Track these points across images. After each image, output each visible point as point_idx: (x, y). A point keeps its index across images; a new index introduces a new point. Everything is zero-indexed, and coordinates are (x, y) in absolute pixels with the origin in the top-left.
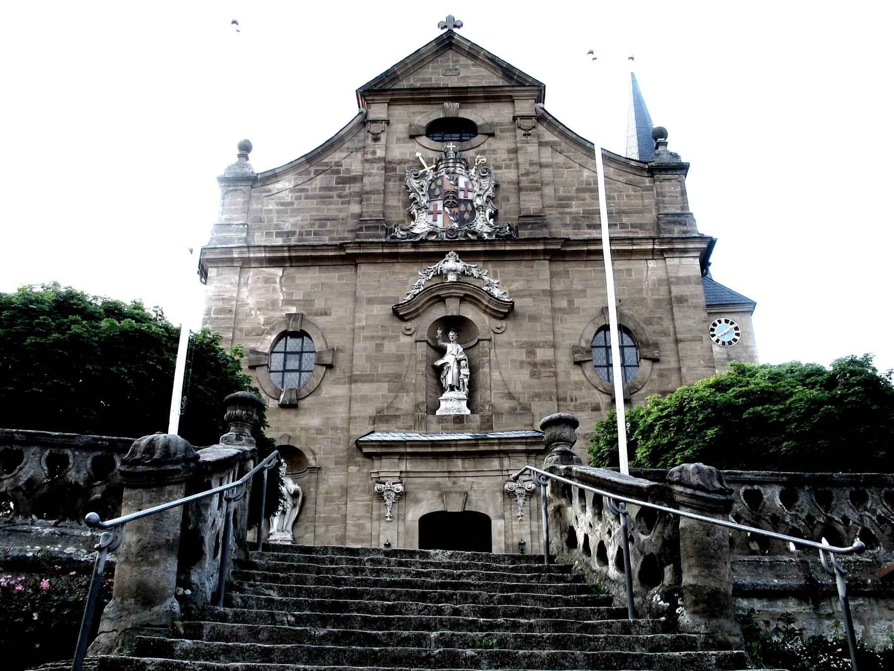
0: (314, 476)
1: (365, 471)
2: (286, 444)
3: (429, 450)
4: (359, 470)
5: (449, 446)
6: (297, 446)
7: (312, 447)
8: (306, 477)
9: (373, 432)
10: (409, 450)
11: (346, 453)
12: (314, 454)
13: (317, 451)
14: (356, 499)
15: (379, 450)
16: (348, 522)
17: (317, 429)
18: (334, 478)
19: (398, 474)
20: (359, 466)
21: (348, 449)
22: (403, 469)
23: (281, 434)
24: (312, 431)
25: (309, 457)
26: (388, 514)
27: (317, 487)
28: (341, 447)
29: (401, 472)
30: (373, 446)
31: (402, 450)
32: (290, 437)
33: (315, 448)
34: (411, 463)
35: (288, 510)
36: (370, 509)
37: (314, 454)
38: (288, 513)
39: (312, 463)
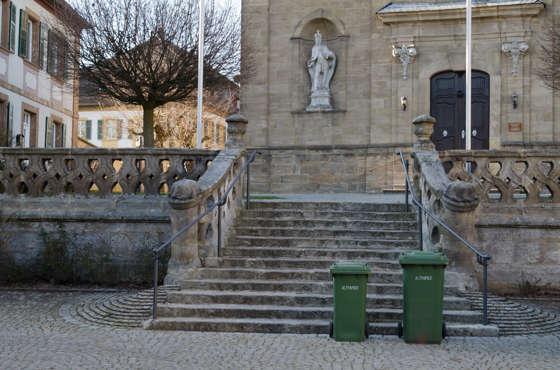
0: (344, 43)
1: (385, 37)
2: (320, 17)
3: (438, 18)
4: (380, 37)
5: (455, 14)
6: (329, 18)
7: (342, 19)
8: (337, 43)
9: (390, 4)
10: (421, 18)
11: (369, 23)
12: (343, 24)
13: (345, 22)
14: (379, 61)
15: (396, 20)
16: (372, 80)
17: (344, 3)
18: (359, 45)
19: (412, 40)
20: (380, 33)
21: (371, 20)
22: (417, 35)
23: (315, 8)
24: (341, 4)
25: (340, 27)
26: (404, 73)
27: (347, 53)
28: (365, 17)
29: (415, 37)
30: (391, 17)
31: (415, 19)
32: (323, 11)
33: (344, 19)
34: (423, 29)
35: (325, 72)
36: (390, 69)
37: (343, 24)
38: (325, 74)
39: (343, 32)
